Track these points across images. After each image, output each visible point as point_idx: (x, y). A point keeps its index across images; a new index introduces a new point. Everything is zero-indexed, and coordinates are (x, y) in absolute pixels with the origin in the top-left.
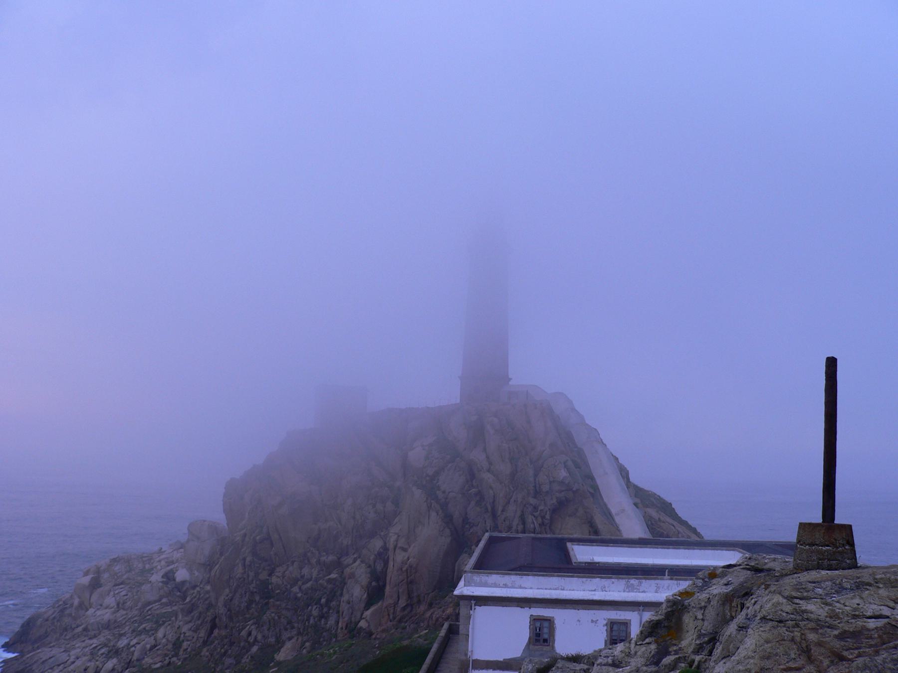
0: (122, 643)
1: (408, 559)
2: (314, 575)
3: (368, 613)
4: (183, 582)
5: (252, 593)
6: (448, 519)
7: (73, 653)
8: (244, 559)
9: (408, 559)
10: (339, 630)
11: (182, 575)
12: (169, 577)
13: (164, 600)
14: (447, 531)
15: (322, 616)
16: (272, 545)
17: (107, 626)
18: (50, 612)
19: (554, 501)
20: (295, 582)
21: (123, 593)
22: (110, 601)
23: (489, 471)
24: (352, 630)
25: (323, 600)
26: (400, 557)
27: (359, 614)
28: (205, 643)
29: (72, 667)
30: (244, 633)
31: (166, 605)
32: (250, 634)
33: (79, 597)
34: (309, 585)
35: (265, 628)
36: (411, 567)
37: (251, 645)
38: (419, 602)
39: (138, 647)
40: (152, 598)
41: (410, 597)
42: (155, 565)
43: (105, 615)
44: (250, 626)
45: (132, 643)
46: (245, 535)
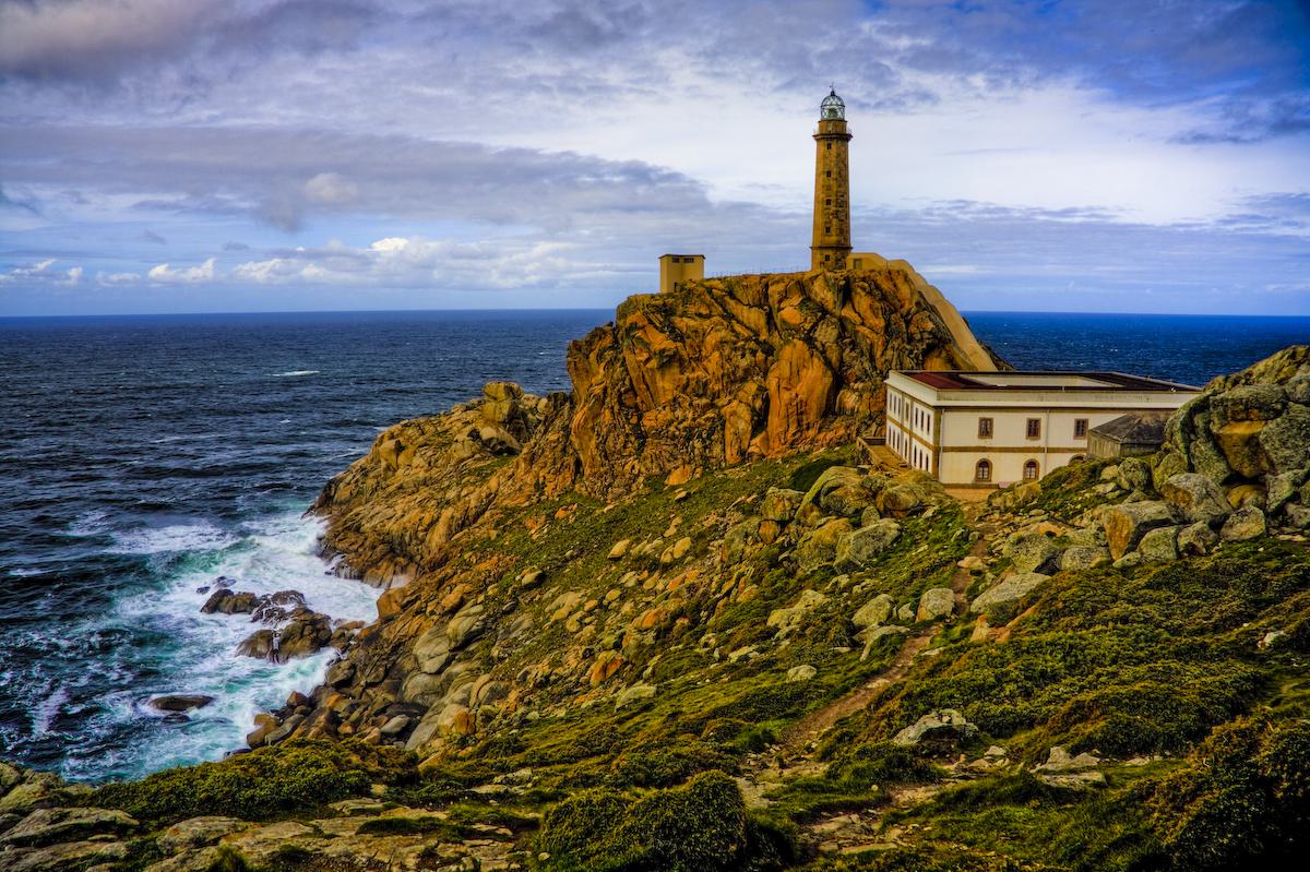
0: (451, 494)
2: (690, 416)
3: (757, 440)
4: (491, 439)
5: (627, 435)
6: (828, 363)
7: (397, 508)
10: (728, 457)
11: (487, 432)
12: (475, 435)
13: (477, 456)
15: (705, 447)
16: (636, 395)
17: (425, 483)
20: (670, 423)
21: (430, 453)
23: (863, 324)
24: (744, 455)
25: (704, 436)
26: (786, 396)
28: (573, 482)
29: (405, 519)
30: (628, 467)
31: (479, 460)
32: (633, 468)
34: (685, 424)
35: (648, 462)
37: (637, 476)
38: (808, 428)
39: (472, 496)
40: (465, 455)
41: (799, 425)
42: (447, 426)
43: (422, 475)
44: (631, 461)
45: (463, 494)
46: (605, 389)
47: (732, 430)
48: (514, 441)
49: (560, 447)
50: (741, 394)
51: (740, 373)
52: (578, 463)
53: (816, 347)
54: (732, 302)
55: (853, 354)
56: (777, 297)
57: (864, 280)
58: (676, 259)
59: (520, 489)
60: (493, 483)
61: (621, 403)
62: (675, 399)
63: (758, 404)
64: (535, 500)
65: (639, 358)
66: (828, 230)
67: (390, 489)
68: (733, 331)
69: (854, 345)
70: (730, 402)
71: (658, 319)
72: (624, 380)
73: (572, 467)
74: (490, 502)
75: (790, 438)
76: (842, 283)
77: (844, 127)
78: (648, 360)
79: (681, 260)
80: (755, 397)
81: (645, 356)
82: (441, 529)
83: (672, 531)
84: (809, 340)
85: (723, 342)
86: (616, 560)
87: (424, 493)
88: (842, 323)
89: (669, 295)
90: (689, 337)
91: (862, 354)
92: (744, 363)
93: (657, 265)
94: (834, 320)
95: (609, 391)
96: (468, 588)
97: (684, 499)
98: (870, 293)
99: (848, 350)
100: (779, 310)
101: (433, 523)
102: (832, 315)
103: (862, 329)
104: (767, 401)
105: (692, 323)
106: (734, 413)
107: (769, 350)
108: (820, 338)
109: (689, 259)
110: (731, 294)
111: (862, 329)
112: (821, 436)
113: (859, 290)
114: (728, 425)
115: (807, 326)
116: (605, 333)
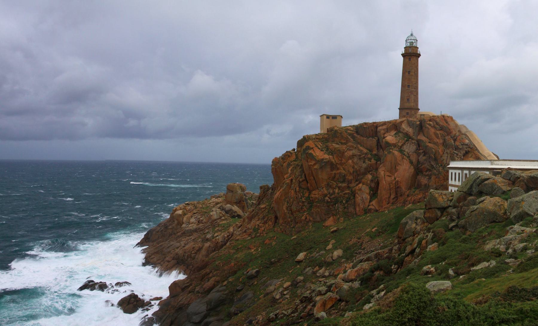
1: (395, 179)
3: (374, 202)
6: (411, 162)
7: (181, 243)
8: (295, 189)
9: (395, 179)
10: (357, 212)
14: (412, 167)
17: (196, 231)
18: (159, 228)
19: (464, 152)
22: (193, 220)
23: (430, 142)
25: (344, 202)
27: (367, 204)
29: (186, 248)
31: (223, 220)
33: (177, 220)
34: (333, 196)
36: (398, 181)
37: (308, 222)
38: (401, 195)
41: (396, 194)
46: (292, 180)
47: (359, 198)
48: (241, 211)
49: (267, 211)
50: (363, 180)
51: (362, 170)
52: (276, 218)
53: (404, 154)
54: (358, 136)
55: (424, 158)
56: (382, 132)
57: (430, 120)
58: (328, 117)
59: (245, 232)
60: (231, 230)
61: (300, 187)
62: (328, 185)
63: (373, 185)
64: (253, 236)
65: (310, 164)
66: (408, 99)
67: (179, 234)
68: (359, 150)
69: (425, 153)
70: (357, 185)
71: (320, 145)
72: (301, 175)
73: (273, 220)
74: (229, 239)
75: (391, 201)
76: (418, 123)
77: (417, 51)
78: (315, 164)
79: (331, 118)
80: (372, 181)
81: (313, 162)
82: (203, 252)
83: (330, 247)
84: (401, 151)
85: (353, 156)
86: (299, 262)
87: (195, 235)
88: (419, 144)
89: (325, 134)
90: (335, 153)
91: (430, 157)
92: (364, 165)
93: (318, 119)
94: (413, 141)
95: (294, 181)
96: (217, 278)
97: (335, 231)
98: (434, 127)
99: (421, 156)
100: (384, 138)
101: (200, 249)
102: (413, 139)
103: (429, 145)
104: (378, 183)
105: (337, 146)
106: (360, 190)
107: (378, 158)
108: (407, 150)
109: (334, 117)
110: (357, 133)
111: (429, 145)
112: (409, 198)
113: (428, 126)
114: (357, 195)
115: (400, 144)
116: (291, 153)
